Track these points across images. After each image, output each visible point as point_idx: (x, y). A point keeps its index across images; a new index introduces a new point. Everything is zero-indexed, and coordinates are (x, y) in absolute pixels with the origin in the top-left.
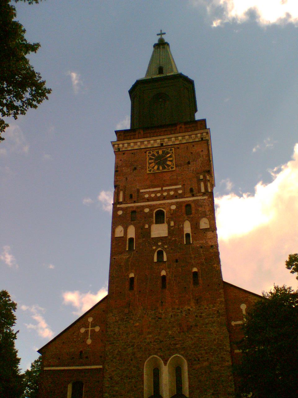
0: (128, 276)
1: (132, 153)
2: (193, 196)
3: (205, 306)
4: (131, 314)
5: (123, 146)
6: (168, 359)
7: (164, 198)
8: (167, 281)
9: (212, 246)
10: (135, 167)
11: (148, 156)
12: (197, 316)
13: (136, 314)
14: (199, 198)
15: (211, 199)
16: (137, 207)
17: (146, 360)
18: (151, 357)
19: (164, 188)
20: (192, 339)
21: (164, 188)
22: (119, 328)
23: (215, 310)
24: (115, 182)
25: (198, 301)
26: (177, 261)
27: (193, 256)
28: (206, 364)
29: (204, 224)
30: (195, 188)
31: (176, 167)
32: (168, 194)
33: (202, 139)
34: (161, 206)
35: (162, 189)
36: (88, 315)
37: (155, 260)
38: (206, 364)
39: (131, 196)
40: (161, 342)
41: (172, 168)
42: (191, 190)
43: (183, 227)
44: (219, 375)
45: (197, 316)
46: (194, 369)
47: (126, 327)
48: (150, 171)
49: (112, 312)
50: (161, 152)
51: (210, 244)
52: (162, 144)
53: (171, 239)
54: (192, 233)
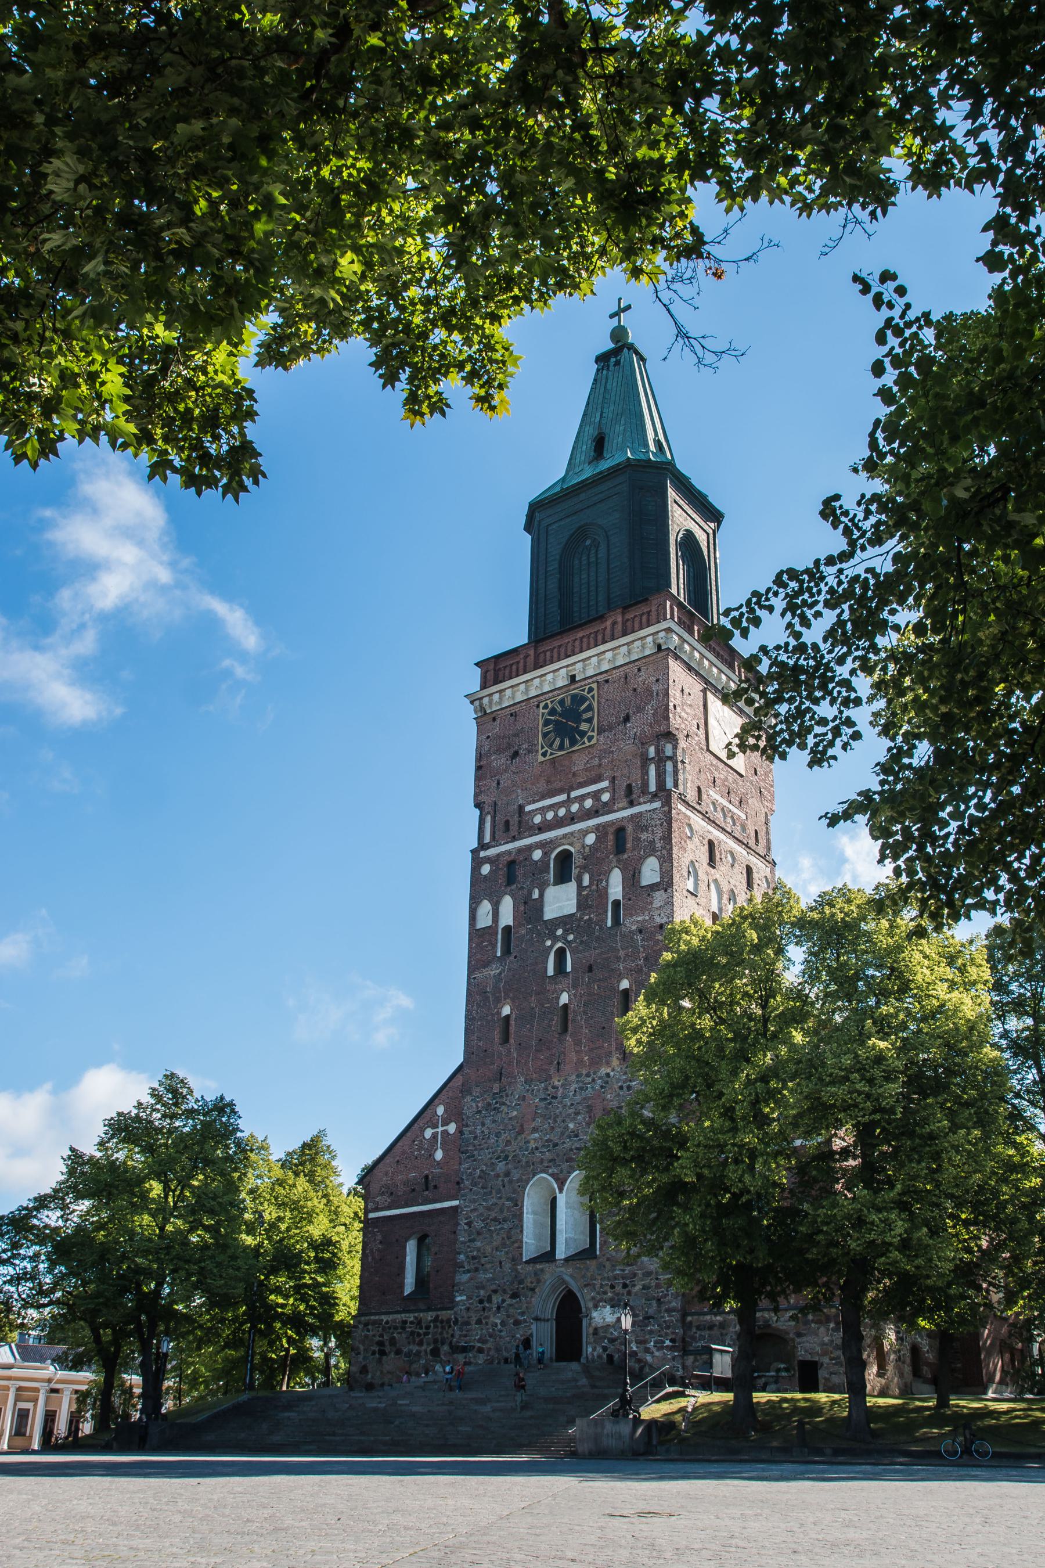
0: (499, 1013)
2: (632, 804)
5: (491, 702)
7: (572, 819)
8: (570, 1017)
9: (661, 926)
12: (621, 1088)
15: (666, 808)
16: (520, 851)
19: (573, 794)
21: (573, 794)
22: (483, 1125)
24: (476, 795)
27: (622, 953)
29: (650, 872)
30: (637, 783)
32: (581, 806)
33: (659, 646)
37: (551, 972)
40: (555, 1145)
41: (590, 738)
42: (629, 789)
47: (494, 1121)
48: (544, 754)
49: (471, 1094)
50: (568, 702)
51: (658, 920)
52: (573, 678)
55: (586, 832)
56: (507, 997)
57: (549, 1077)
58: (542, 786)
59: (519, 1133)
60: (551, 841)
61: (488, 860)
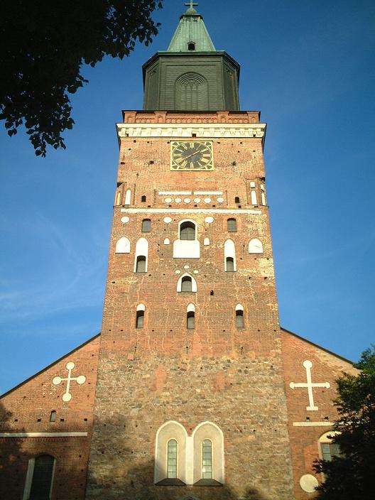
1: (148, 142)
2: (240, 207)
3: (253, 359)
4: (138, 362)
6: (194, 428)
9: (266, 278)
10: (152, 160)
11: (173, 147)
12: (240, 371)
13: (146, 362)
14: (249, 212)
16: (154, 215)
17: (159, 427)
18: (167, 423)
20: (231, 401)
21: (195, 193)
22: (118, 380)
23: (267, 365)
25: (243, 350)
26: (212, 293)
27: (236, 288)
28: (251, 437)
29: (255, 246)
31: (215, 166)
32: (202, 202)
34: (188, 217)
35: (193, 193)
36: (67, 359)
37: (179, 289)
38: (251, 437)
39: (144, 199)
40: (184, 402)
41: (209, 167)
42: (237, 200)
43: (223, 249)
44: (271, 454)
45: (240, 371)
46: (233, 444)
47: (129, 379)
48: (175, 167)
52: (194, 135)
53: (204, 263)
54: (237, 257)
55: (207, 216)
56: (142, 298)
57: (178, 356)
58: (172, 183)
59: (151, 390)
60: (179, 215)
61: (128, 215)
